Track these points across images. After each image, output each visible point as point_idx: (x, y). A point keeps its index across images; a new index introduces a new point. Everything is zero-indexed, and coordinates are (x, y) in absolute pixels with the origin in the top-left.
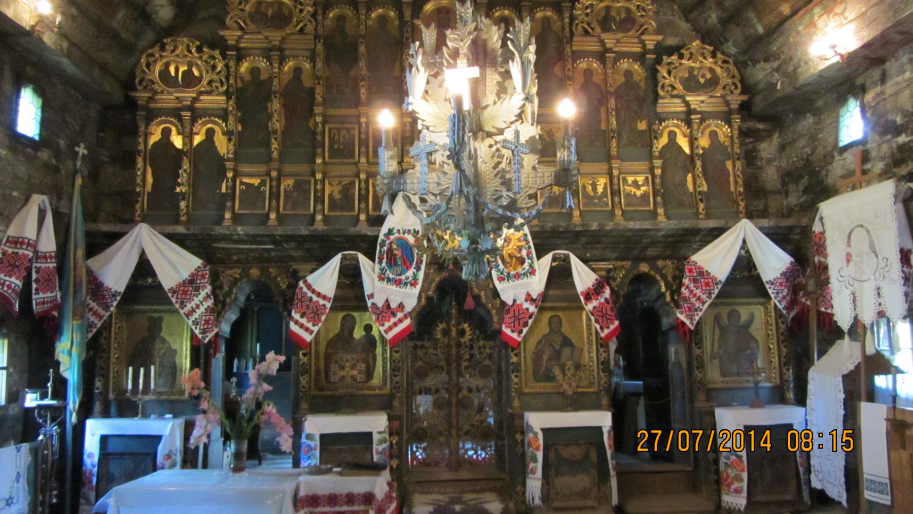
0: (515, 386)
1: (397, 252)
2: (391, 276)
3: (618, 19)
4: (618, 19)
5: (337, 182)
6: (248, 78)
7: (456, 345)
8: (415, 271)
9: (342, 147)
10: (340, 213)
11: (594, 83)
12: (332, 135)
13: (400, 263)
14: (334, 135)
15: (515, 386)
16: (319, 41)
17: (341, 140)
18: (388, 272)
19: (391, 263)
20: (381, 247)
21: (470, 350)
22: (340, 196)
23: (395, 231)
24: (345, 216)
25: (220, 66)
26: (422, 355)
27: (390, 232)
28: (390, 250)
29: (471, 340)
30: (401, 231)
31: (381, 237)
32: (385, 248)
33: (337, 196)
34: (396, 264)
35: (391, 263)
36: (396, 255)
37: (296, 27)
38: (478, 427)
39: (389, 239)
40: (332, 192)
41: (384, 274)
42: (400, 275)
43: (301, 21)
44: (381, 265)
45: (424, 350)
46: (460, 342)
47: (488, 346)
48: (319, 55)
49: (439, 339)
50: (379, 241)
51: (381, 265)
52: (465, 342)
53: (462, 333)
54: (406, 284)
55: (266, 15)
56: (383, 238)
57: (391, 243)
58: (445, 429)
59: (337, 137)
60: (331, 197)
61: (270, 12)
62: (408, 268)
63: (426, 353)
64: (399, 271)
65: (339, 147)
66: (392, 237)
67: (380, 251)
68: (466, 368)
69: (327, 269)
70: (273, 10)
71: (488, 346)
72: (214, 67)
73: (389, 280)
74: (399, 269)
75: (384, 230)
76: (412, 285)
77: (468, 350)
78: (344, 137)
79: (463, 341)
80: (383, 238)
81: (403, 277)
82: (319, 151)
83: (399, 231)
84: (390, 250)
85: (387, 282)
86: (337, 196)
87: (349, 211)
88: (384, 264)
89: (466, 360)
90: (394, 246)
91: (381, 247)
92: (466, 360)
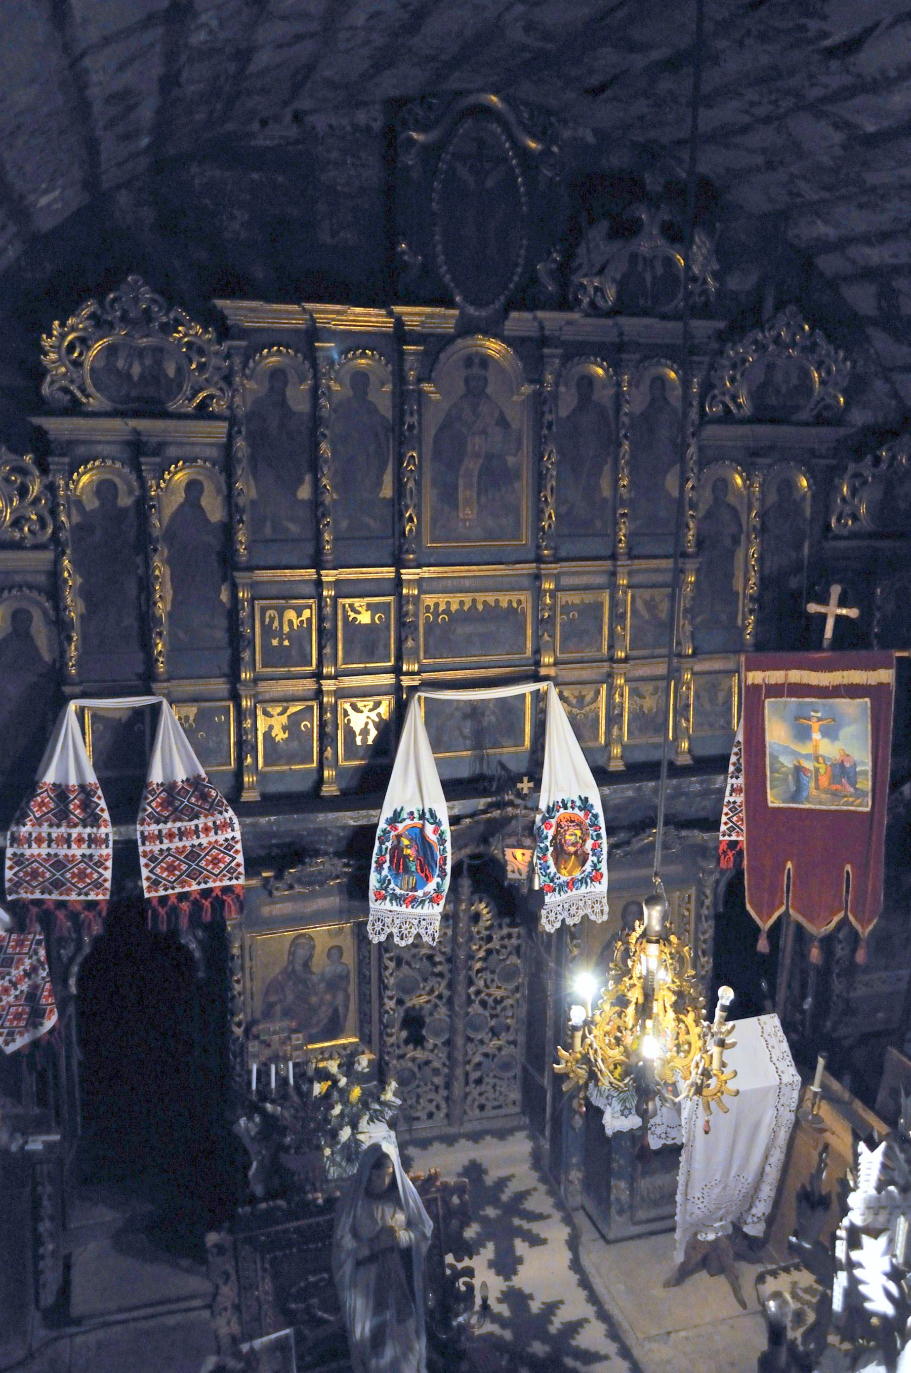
1: (409, 851)
2: (398, 891)
3: (784, 390)
4: (784, 390)
5: (279, 709)
6: (92, 504)
8: (439, 880)
9: (286, 643)
10: (286, 768)
11: (729, 505)
12: (267, 620)
13: (413, 869)
14: (272, 620)
16: (239, 432)
17: (286, 629)
18: (392, 886)
19: (398, 868)
20: (382, 843)
22: (286, 735)
23: (404, 815)
24: (296, 771)
25: (35, 489)
27: (396, 818)
28: (397, 849)
30: (416, 815)
31: (382, 825)
32: (389, 845)
33: (280, 735)
34: (407, 870)
35: (398, 868)
36: (408, 856)
37: (190, 400)
38: (494, 1056)
39: (396, 829)
40: (271, 727)
41: (385, 889)
42: (415, 889)
43: (201, 390)
44: (380, 873)
47: (515, 935)
48: (239, 461)
50: (379, 832)
51: (380, 873)
52: (478, 933)
53: (476, 918)
54: (423, 902)
55: (129, 376)
56: (385, 826)
57: (399, 837)
58: (444, 1065)
59: (276, 624)
60: (267, 735)
61: (136, 370)
62: (428, 879)
64: (412, 881)
65: (281, 642)
66: (401, 827)
67: (380, 849)
68: (478, 971)
69: (166, 720)
70: (142, 364)
71: (515, 935)
72: (23, 491)
73: (395, 897)
74: (412, 881)
75: (387, 812)
76: (432, 900)
78: (290, 622)
79: (474, 929)
80: (385, 826)
81: (420, 893)
82: (246, 655)
83: (412, 813)
84: (397, 849)
85: (391, 900)
86: (280, 735)
87: (302, 762)
88: (385, 872)
89: (480, 959)
90: (406, 842)
91: (382, 843)
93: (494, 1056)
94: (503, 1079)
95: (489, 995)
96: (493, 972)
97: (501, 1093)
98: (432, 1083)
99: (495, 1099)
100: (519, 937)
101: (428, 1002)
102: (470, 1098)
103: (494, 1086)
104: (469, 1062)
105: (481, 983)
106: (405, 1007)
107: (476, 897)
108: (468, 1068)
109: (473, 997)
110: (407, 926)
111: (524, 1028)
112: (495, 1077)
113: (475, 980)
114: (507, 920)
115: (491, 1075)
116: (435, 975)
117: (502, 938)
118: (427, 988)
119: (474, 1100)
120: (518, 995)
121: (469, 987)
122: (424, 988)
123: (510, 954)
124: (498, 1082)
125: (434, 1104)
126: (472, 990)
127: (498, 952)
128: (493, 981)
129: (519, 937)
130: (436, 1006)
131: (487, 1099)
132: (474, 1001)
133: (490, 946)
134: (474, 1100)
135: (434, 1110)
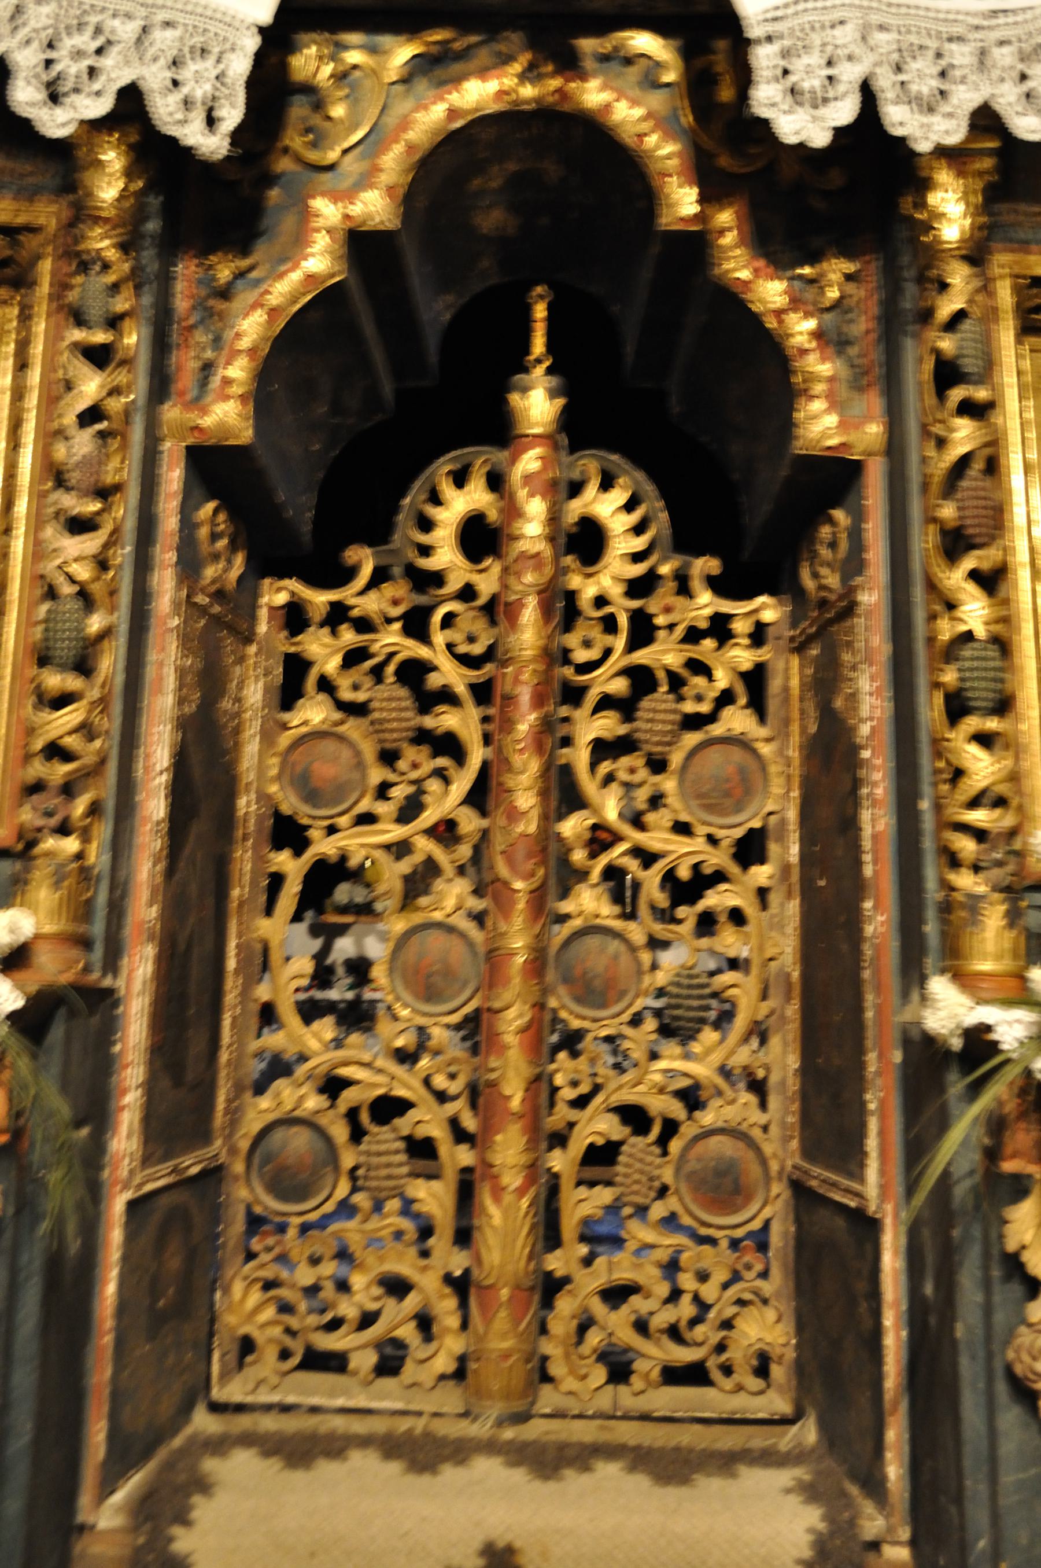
0: (979, 817)
7: (546, 610)
15: (979, 817)
21: (633, 645)
26: (332, 665)
29: (639, 587)
45: (348, 636)
46: (571, 596)
49: (437, 579)
52: (601, 601)
63: (353, 658)
68: (602, 749)
71: (741, 627)
77: (620, 643)
79: (589, 591)
89: (606, 703)
92: (606, 703)
93: (670, 1128)
94: (712, 1241)
95: (647, 858)
96: (658, 765)
97: (703, 1306)
98: (407, 1208)
99: (674, 1333)
100: (759, 635)
101: (400, 849)
102: (565, 1305)
103: (672, 1267)
104: (559, 1139)
105: (611, 808)
106: (310, 855)
107: (589, 464)
108: (558, 1161)
109: (579, 856)
110: (85, 41)
111: (793, 1010)
112: (670, 1221)
113: (589, 785)
114: (706, 565)
115: (658, 1210)
116: (422, 737)
117: (693, 636)
118: (399, 792)
119: (585, 1325)
120: (762, 874)
121: (561, 817)
122: (382, 791)
123: (726, 698)
124: (691, 1255)
125: (412, 1302)
126: (573, 826)
127: (676, 682)
128: (656, 801)
129: (759, 635)
130: (430, 869)
131: (641, 1326)
132: (583, 875)
133: (642, 656)
134: (585, 1325)
135: (408, 1332)
